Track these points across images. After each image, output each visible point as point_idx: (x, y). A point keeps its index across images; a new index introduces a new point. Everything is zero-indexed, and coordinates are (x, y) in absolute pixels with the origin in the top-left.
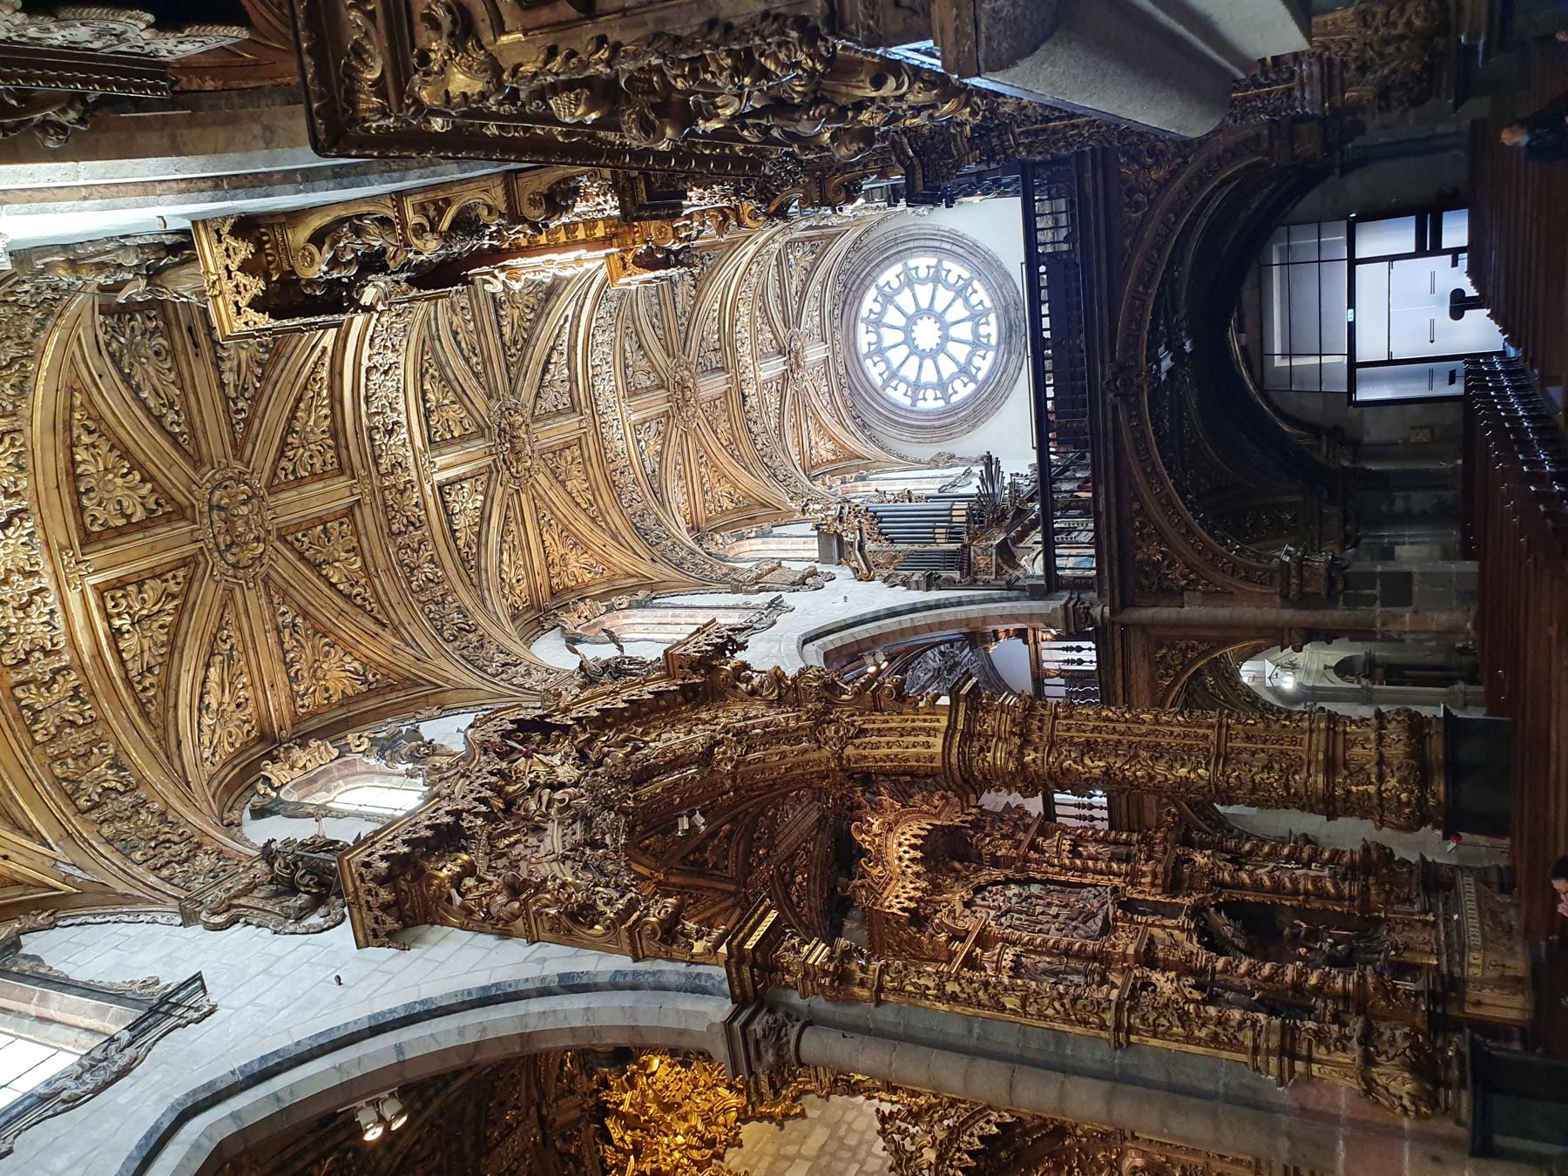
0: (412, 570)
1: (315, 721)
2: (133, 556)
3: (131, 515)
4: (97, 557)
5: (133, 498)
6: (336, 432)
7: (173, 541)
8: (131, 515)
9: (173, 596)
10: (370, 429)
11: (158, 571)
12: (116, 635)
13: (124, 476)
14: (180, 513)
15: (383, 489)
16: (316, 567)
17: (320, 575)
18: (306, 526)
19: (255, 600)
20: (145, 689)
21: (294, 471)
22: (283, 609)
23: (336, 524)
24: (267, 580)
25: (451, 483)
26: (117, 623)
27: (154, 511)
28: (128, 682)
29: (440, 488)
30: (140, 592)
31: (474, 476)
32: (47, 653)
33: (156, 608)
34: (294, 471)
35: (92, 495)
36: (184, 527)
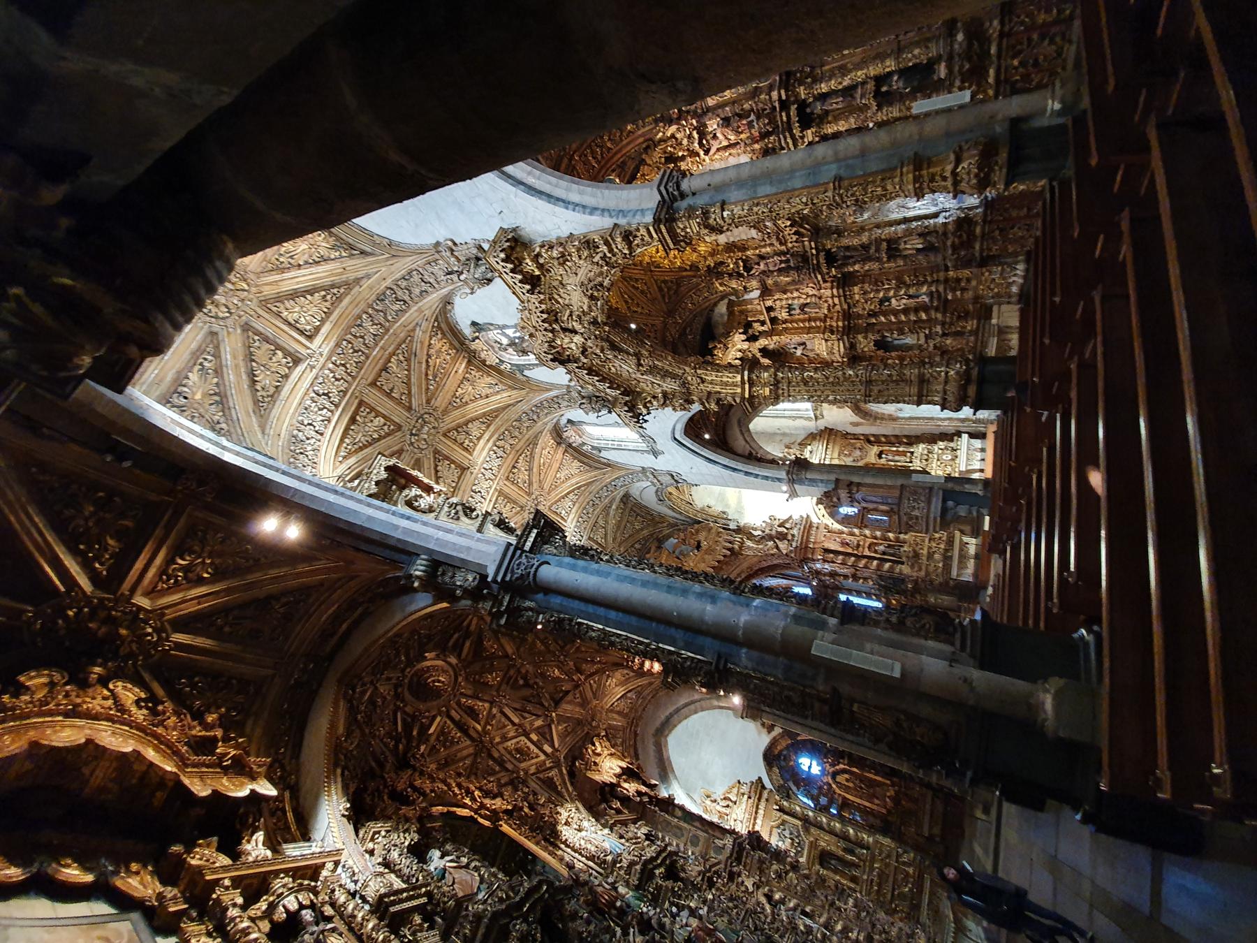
0: (375, 335)
2: (458, 454)
4: (466, 463)
6: (353, 420)
7: (447, 447)
10: (337, 406)
12: (479, 439)
14: (436, 452)
15: (354, 378)
16: (408, 384)
17: (409, 379)
18: (398, 402)
19: (440, 401)
21: (385, 425)
23: (385, 387)
24: (428, 402)
25: (301, 332)
28: (488, 427)
29: (310, 338)
31: (278, 315)
34: (385, 425)
36: (440, 447)
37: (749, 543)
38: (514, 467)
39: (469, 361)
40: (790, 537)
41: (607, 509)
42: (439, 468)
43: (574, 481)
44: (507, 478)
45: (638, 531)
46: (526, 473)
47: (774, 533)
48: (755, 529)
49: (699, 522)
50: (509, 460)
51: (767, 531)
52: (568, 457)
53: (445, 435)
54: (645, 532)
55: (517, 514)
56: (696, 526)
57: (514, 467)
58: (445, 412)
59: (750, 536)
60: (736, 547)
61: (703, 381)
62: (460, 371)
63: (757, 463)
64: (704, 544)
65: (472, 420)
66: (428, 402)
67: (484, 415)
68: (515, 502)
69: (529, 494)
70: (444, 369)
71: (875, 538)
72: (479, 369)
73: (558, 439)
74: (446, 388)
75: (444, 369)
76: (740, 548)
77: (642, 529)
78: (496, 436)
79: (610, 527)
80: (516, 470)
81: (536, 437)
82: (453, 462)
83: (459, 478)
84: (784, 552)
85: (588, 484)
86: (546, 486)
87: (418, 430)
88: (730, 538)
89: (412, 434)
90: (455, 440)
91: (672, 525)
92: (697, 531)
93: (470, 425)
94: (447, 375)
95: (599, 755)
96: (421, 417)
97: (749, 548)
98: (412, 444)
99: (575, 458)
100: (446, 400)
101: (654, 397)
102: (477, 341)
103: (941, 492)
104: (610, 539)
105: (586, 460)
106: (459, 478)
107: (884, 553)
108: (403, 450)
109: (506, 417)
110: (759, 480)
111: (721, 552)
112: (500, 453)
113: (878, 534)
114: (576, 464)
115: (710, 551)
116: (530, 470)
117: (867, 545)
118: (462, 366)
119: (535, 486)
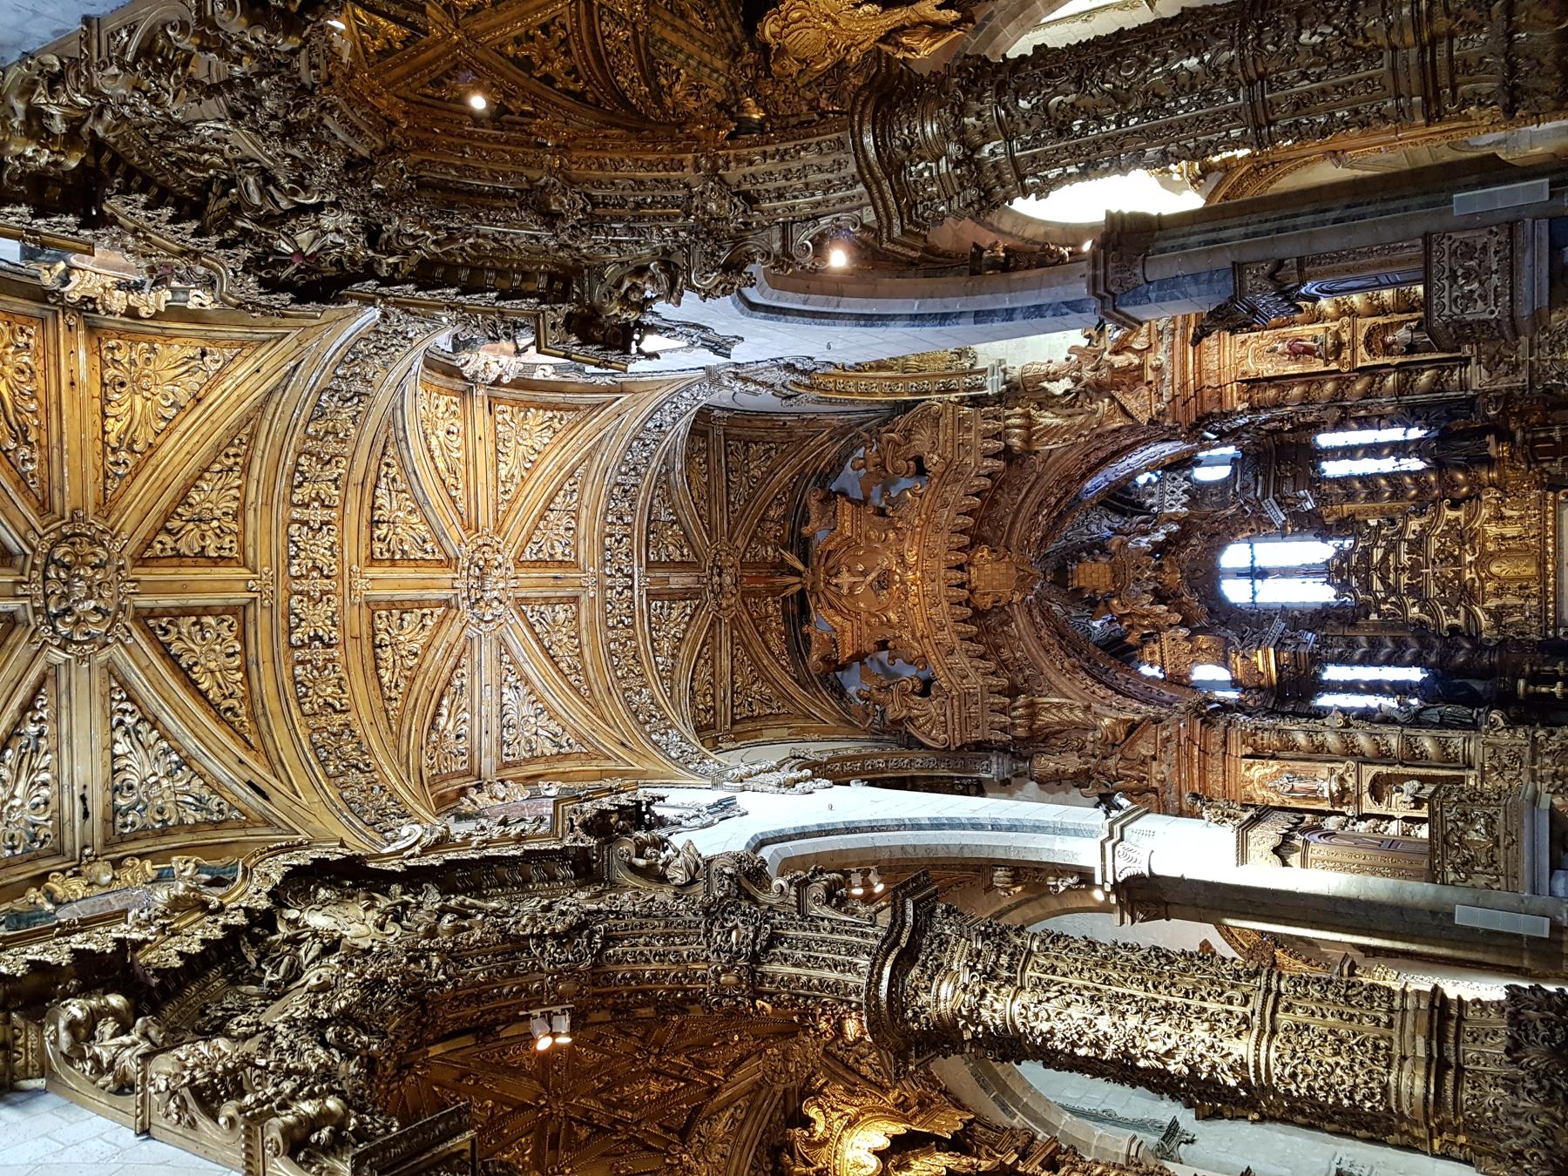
1: (15, 308)
3: (194, 624)
5: (185, 639)
8: (194, 624)
9: (169, 532)
11: (175, 561)
13: (196, 664)
14: (143, 617)
20: (236, 456)
22: (30, 467)
26: (234, 526)
27: (169, 623)
28: (246, 470)
30: (203, 548)
32: (306, 523)
33: (191, 526)
35: (231, 650)
37: (1048, 419)
38: (374, 524)
39: (91, 329)
40: (1150, 376)
41: (663, 479)
42: (174, 650)
43: (548, 466)
44: (372, 560)
45: (762, 481)
46: (414, 519)
47: (1105, 373)
48: (1054, 377)
49: (908, 406)
50: (352, 507)
51: (1087, 375)
52: (505, 412)
53: (141, 561)
54: (784, 475)
55: (440, 623)
56: (902, 421)
57: (374, 524)
58: (106, 505)
59: (1047, 401)
60: (1016, 442)
61: (751, 200)
62: (83, 373)
63: (1000, 279)
64: (933, 461)
65: (192, 484)
66: (44, 507)
67: (218, 450)
68: (420, 604)
69: (449, 562)
70: (33, 396)
71: (1382, 310)
72: (132, 336)
73: (459, 384)
74: (71, 443)
75: (33, 396)
76: (1027, 441)
77: (771, 471)
78: (282, 484)
79: (685, 515)
80: (382, 531)
81: (392, 423)
82: (207, 610)
83: (242, 638)
84: (1144, 418)
85: (589, 455)
86: (485, 518)
87: (65, 596)
88: (991, 425)
89: (52, 619)
90: (179, 555)
91: (843, 431)
92: (908, 434)
93: (195, 497)
94: (52, 407)
95: (824, 1142)
96: (50, 560)
97: (1050, 431)
98: (69, 640)
99: (526, 406)
100: (91, 474)
101: (641, 271)
102: (75, 278)
103: (1544, 225)
104: (700, 538)
105: (557, 398)
106: (242, 638)
107: (1411, 348)
108: (51, 666)
109: (279, 426)
110: (1019, 322)
111: (978, 465)
112: (317, 515)
113: (1387, 295)
114: (536, 418)
115: (953, 472)
116: (420, 506)
117: (1361, 337)
118: (79, 360)
119: (455, 533)
